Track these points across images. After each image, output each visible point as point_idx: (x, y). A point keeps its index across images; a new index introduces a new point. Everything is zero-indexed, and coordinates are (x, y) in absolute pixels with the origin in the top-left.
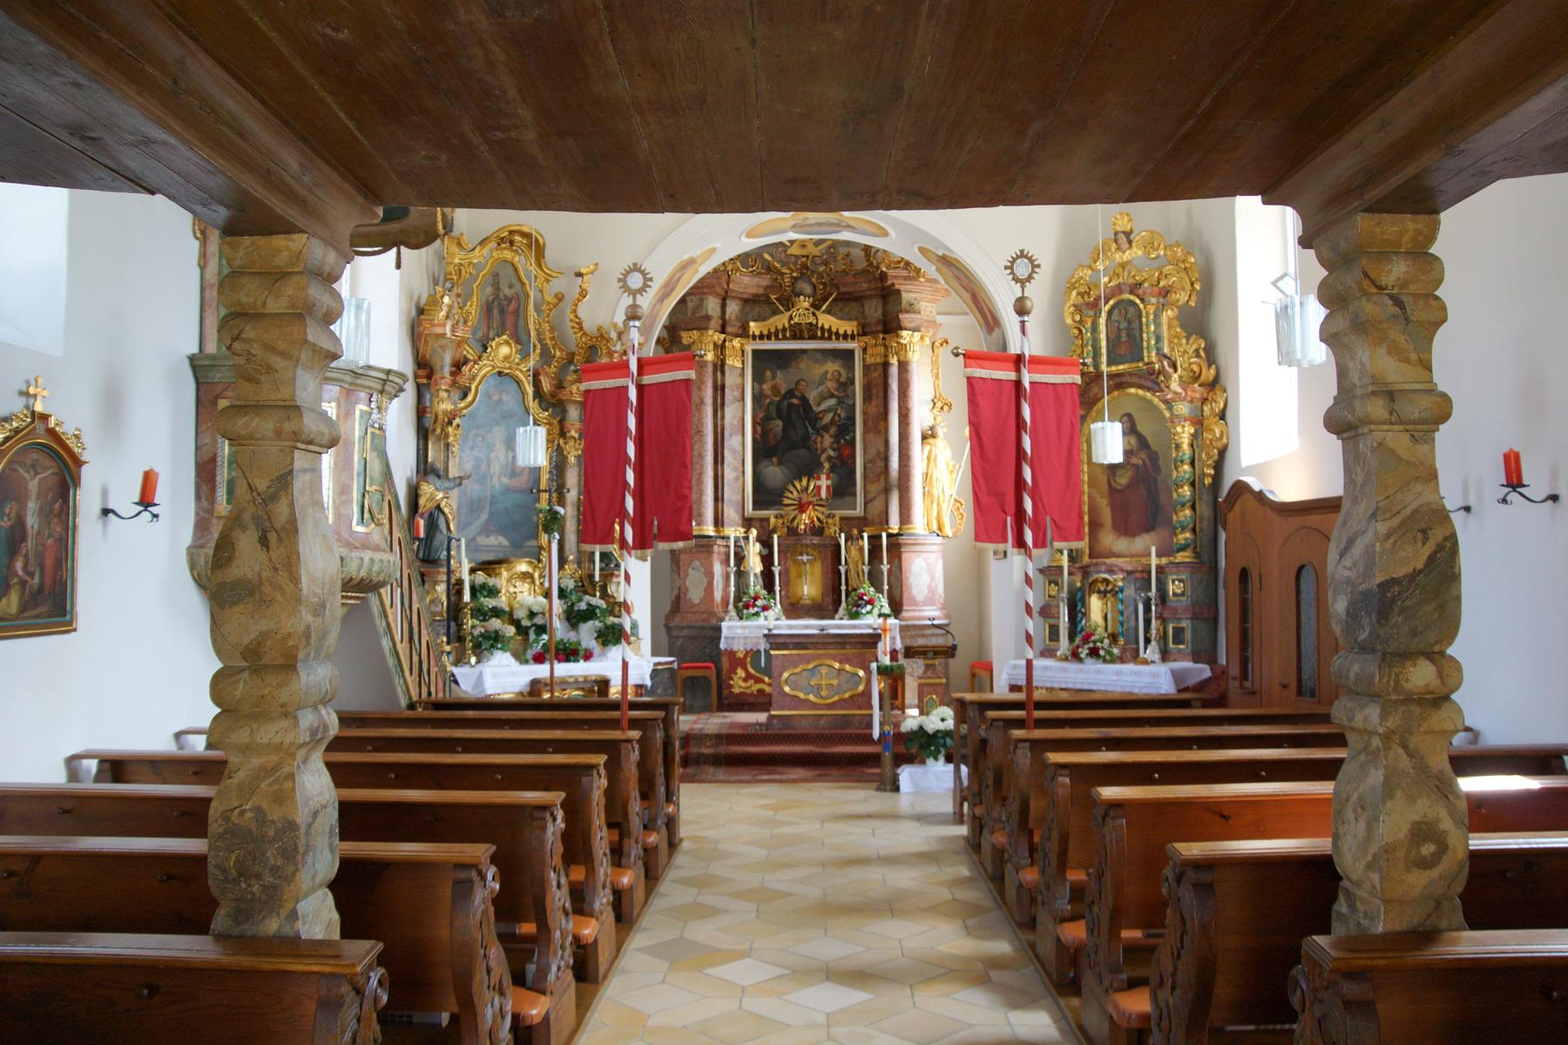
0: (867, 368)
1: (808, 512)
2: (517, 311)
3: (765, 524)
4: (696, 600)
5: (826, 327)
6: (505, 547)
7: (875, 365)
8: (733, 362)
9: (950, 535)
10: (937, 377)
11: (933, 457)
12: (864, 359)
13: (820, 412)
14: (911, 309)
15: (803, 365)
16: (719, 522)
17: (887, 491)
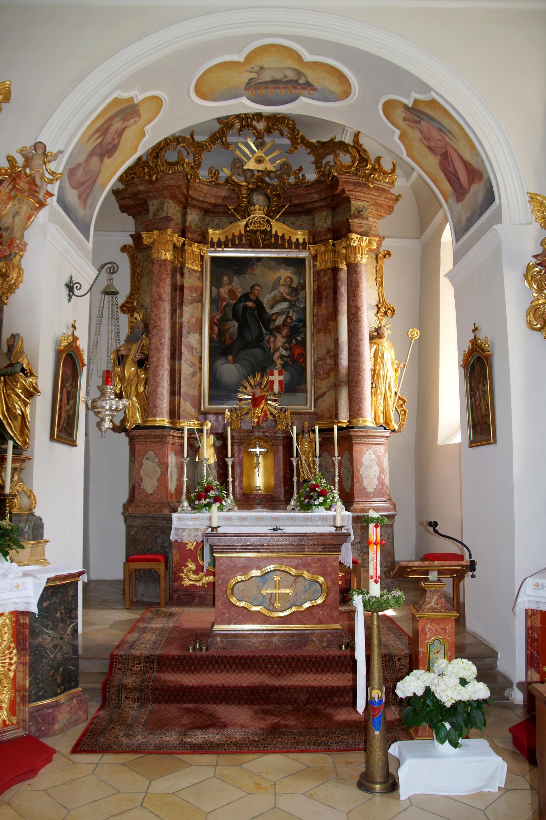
0: (317, 274)
1: (262, 406)
3: (220, 417)
4: (150, 491)
5: (280, 234)
7: (325, 270)
8: (192, 265)
9: (396, 427)
10: (380, 284)
11: (380, 355)
12: (314, 266)
13: (273, 314)
14: (359, 214)
15: (257, 271)
16: (174, 414)
17: (336, 386)
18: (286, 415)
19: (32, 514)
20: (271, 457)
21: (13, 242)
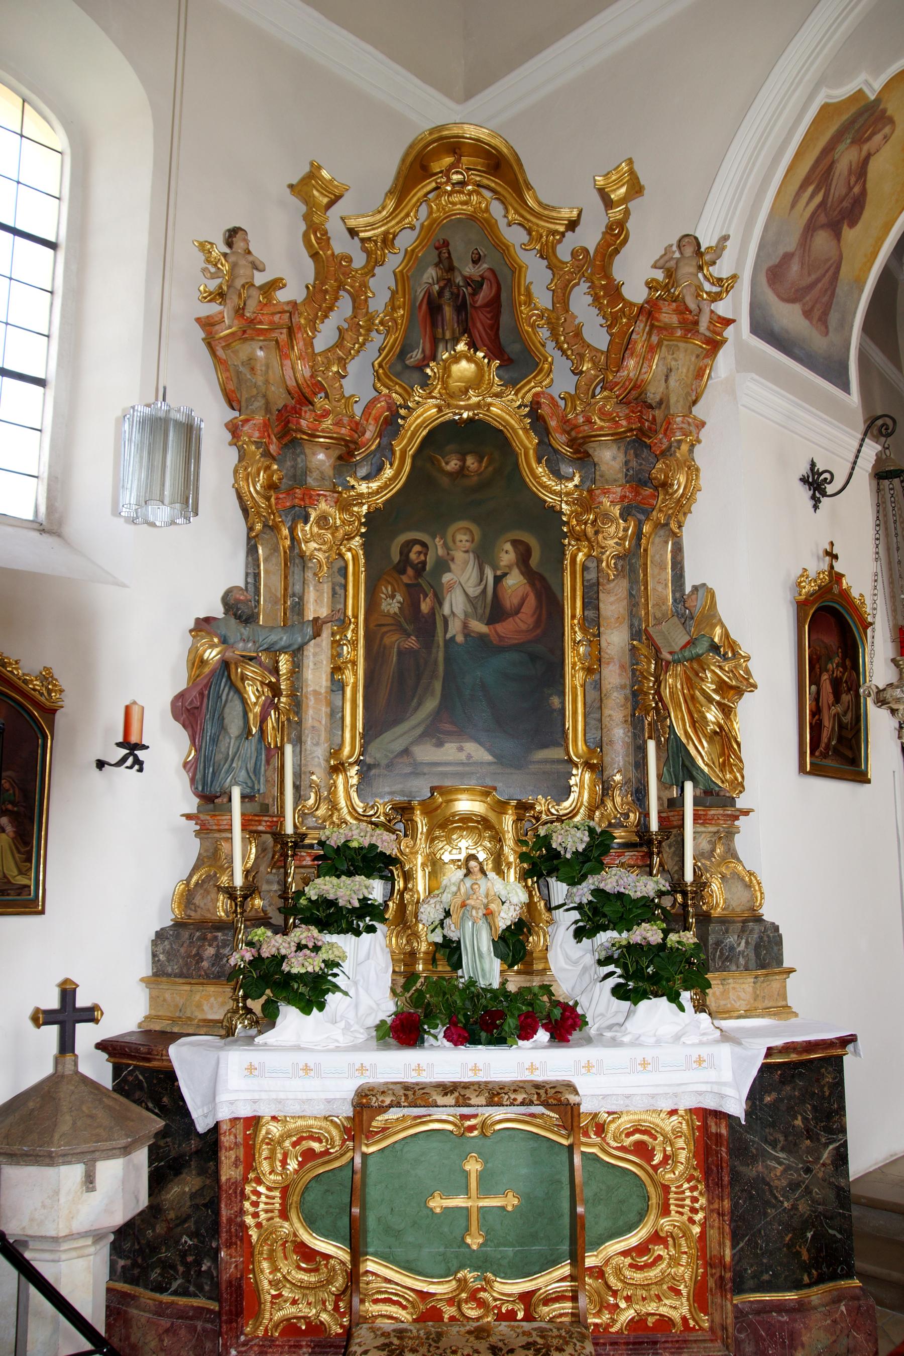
2: (495, 304)
6: (490, 764)
19: (759, 919)
21: (670, 423)
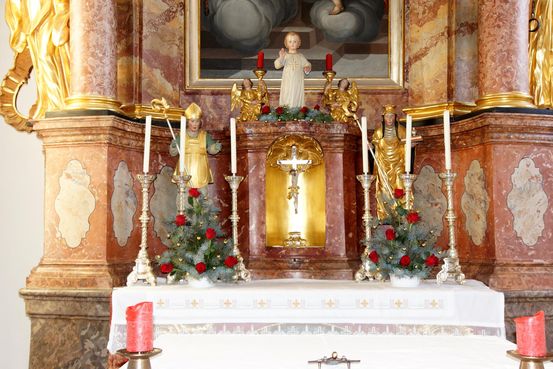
3: (222, 100)
18: (348, 95)
20: (321, 173)
